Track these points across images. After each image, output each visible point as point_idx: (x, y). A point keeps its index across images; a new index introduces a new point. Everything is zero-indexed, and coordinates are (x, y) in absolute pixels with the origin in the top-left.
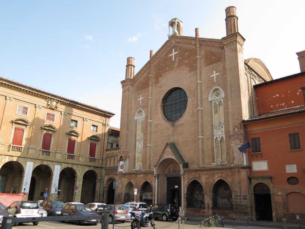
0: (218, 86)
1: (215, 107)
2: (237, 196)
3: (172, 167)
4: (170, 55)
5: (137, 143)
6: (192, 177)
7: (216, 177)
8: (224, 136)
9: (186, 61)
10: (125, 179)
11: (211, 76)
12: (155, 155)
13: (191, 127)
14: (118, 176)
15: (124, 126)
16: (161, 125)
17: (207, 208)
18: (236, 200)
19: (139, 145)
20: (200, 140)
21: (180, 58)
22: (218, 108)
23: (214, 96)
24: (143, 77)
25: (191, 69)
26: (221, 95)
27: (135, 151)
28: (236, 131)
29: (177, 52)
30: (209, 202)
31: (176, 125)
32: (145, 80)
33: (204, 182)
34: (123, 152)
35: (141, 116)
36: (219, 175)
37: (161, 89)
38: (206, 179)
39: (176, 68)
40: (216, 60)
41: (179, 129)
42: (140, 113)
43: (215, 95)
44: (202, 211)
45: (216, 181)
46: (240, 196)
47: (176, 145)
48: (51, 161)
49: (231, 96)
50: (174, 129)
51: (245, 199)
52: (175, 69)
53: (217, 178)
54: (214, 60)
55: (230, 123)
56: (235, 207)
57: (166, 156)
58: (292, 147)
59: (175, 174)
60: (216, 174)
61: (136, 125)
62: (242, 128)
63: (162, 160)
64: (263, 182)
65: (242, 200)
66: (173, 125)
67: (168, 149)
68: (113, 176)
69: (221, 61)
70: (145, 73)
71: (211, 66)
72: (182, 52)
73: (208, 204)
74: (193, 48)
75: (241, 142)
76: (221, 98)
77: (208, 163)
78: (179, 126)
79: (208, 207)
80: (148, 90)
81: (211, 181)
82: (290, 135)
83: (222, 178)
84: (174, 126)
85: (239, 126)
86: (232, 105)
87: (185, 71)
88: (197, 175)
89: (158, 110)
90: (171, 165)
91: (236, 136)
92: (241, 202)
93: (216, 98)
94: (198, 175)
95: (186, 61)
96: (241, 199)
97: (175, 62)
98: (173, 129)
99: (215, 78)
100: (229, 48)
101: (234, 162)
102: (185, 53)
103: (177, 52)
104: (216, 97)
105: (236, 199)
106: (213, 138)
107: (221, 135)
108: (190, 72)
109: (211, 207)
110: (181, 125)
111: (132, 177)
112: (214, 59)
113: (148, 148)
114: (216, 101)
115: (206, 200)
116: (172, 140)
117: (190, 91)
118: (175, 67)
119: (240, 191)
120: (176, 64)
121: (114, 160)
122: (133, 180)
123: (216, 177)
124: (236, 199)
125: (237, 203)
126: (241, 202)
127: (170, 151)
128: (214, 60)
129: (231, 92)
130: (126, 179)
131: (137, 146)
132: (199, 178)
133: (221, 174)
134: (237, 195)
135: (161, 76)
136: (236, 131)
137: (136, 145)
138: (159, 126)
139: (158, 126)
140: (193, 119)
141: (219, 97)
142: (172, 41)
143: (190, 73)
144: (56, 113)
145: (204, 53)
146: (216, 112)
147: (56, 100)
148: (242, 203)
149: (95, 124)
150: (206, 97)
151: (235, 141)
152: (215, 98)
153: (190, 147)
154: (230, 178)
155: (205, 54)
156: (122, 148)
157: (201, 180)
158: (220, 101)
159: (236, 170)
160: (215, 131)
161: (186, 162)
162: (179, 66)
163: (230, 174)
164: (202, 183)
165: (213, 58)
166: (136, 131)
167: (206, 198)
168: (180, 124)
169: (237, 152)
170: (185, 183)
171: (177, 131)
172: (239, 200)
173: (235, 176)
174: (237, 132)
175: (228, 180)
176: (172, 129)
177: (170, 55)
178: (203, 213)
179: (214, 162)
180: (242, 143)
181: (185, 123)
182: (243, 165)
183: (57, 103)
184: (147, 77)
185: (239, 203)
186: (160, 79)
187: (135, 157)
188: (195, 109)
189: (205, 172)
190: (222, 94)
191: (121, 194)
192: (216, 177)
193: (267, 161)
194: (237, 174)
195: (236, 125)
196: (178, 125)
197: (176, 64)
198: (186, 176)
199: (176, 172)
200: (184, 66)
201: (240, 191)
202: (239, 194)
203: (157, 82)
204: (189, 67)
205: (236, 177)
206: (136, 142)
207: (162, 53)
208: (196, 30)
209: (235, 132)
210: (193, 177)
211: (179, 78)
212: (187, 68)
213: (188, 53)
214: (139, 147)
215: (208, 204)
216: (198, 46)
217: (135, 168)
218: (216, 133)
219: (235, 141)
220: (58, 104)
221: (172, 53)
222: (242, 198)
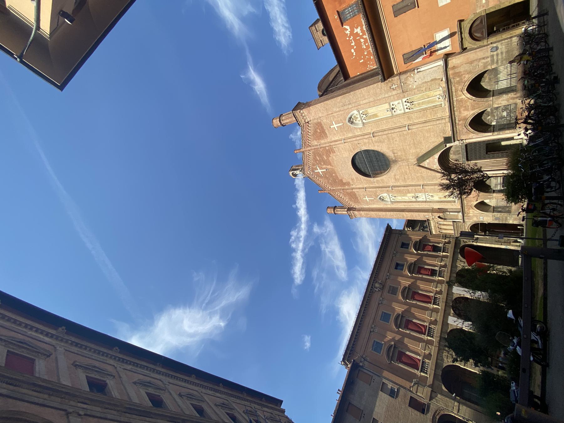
1: (370, 119)
2: (492, 61)
4: (321, 174)
6: (465, 128)
7: (464, 97)
9: (325, 157)
11: (336, 129)
12: (434, 178)
13: (396, 141)
15: (399, 215)
16: (395, 175)
19: (422, 198)
23: (357, 121)
25: (332, 152)
29: (318, 168)
30: (504, 98)
31: (394, 159)
33: (472, 112)
34: (432, 216)
36: (460, 93)
37: (355, 179)
38: (466, 109)
39: (332, 166)
40: (320, 127)
41: (399, 154)
46: (493, 57)
47: (420, 155)
48: (447, 296)
51: (497, 48)
52: (334, 168)
55: (387, 95)
57: (437, 166)
58: (413, 7)
59: (461, 151)
60: (458, 98)
61: (397, 202)
62: (392, 80)
64: (467, 31)
65: (499, 51)
66: (395, 161)
67: (426, 163)
68: (467, 226)
69: (320, 122)
71: (326, 131)
73: (508, 100)
75: (411, 76)
78: (396, 155)
80: (358, 192)
83: (464, 89)
84: (395, 161)
85: (390, 84)
86: (365, 99)
89: (378, 181)
91: (402, 84)
94: (461, 122)
95: (325, 157)
98: (400, 161)
100: (307, 117)
101: (439, 79)
102: (318, 160)
103: (318, 168)
104: (358, 119)
105: (497, 61)
106: (407, 112)
107: (403, 104)
108: (335, 152)
109: (512, 95)
110: (394, 153)
112: (320, 130)
117: (354, 149)
118: (332, 167)
119: (484, 58)
120: (329, 167)
121: (444, 225)
122: (472, 203)
124: (497, 61)
126: (502, 53)
127: (427, 161)
129: (350, 104)
131: (425, 200)
133: (459, 91)
134: (491, 60)
135: (341, 180)
136: (396, 86)
138: (397, 177)
139: (396, 178)
140: (386, 141)
144: (388, 283)
146: (375, 115)
147: (373, 282)
148: (504, 50)
149: (400, 244)
150: (359, 130)
151: (410, 85)
152: (359, 121)
153: (422, 139)
155: (316, 140)
156: (427, 216)
157: (469, 116)
160: (398, 112)
161: (443, 140)
162: (330, 164)
164: (474, 114)
165: (319, 131)
166: (405, 202)
168: (393, 155)
169: (425, 78)
171: (401, 156)
172: (500, 57)
173: (460, 72)
174: (398, 85)
175: (468, 78)
176: (400, 162)
177: (321, 174)
179: (441, 104)
180: (412, 75)
182: (442, 65)
183: (376, 282)
185: (504, 55)
186: (344, 181)
188: (373, 140)
191: (495, 216)
192: (464, 97)
193: (434, 34)
194: (457, 70)
195: (389, 88)
197: (329, 167)
198: (463, 137)
199: (458, 151)
200: (330, 158)
201: (484, 58)
202: (489, 59)
203: (348, 184)
204: (330, 153)
206: (419, 202)
209: (398, 86)
210: (464, 127)
211: (341, 162)
213: (317, 157)
214: (426, 197)
215: (508, 100)
216: (309, 148)
218: (400, 110)
219: (410, 85)
220: (378, 281)
221: (319, 172)
222: (495, 53)
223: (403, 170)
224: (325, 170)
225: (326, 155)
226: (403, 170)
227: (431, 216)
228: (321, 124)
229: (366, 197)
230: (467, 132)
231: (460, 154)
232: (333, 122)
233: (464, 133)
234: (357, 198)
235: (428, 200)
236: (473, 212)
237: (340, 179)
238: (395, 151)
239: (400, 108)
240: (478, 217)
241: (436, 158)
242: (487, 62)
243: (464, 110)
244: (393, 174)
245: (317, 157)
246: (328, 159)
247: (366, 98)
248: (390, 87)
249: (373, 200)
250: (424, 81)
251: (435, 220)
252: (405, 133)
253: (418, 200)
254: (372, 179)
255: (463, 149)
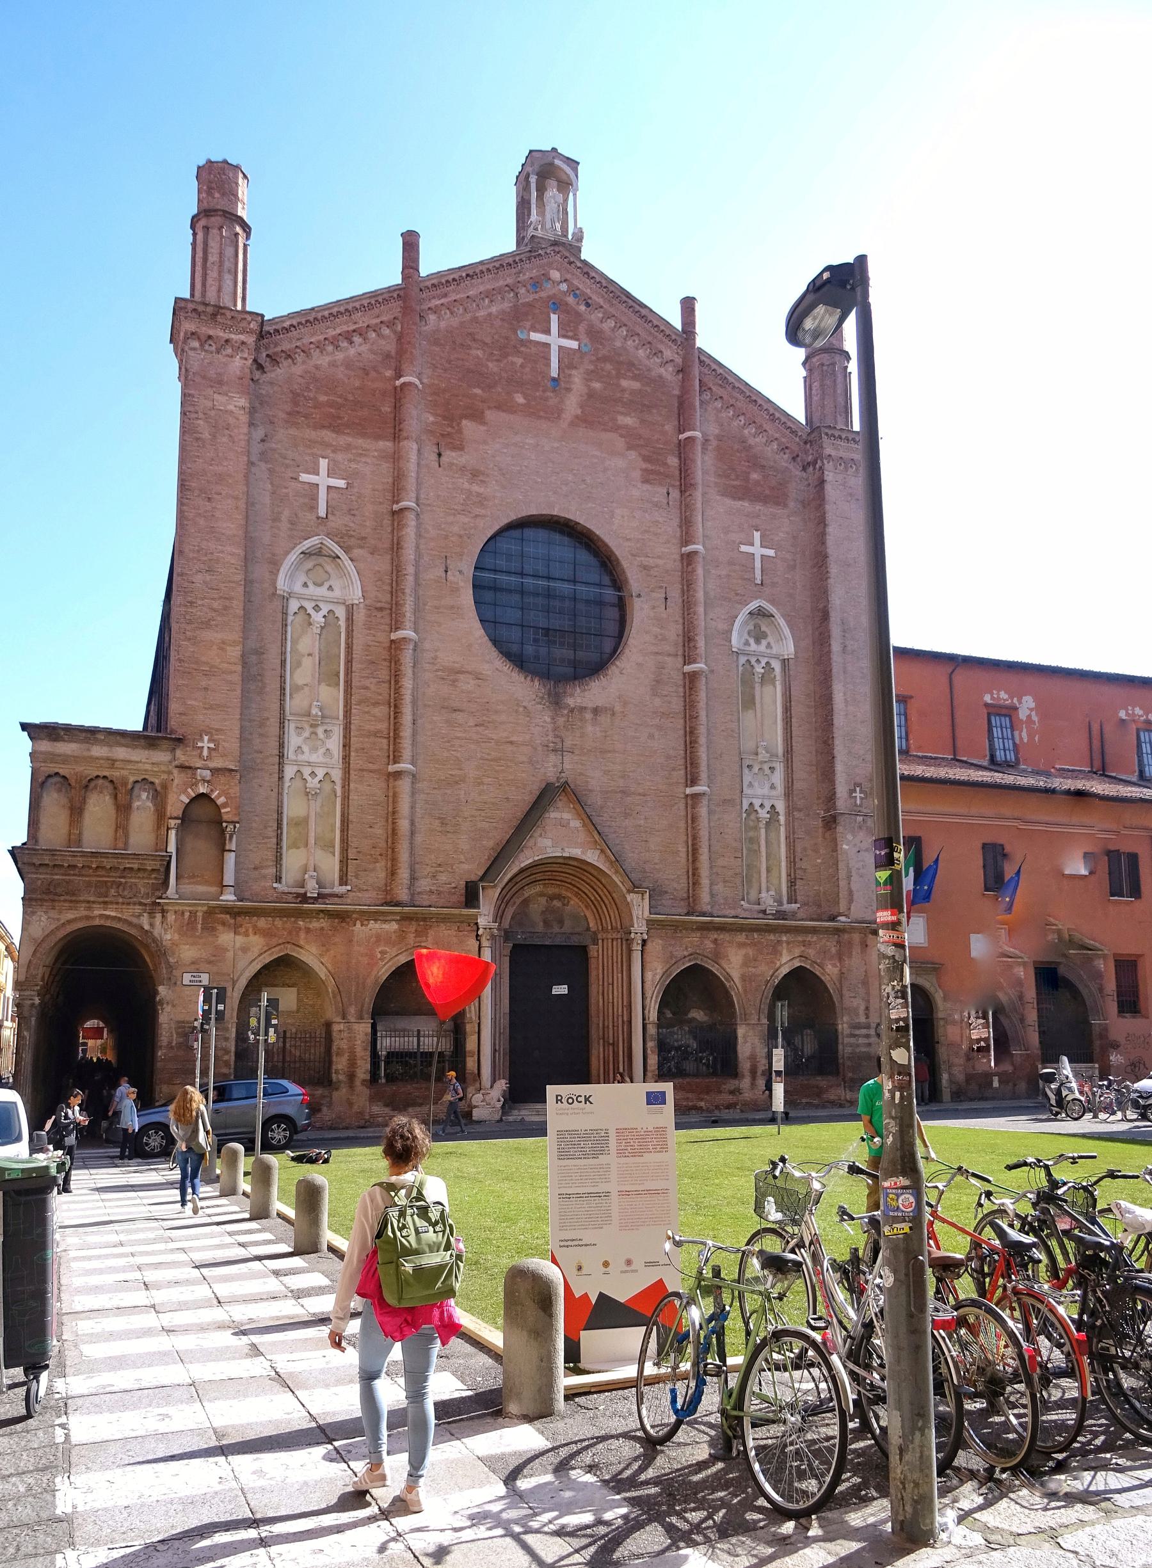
0: (772, 602)
2: (858, 1026)
3: (543, 900)
5: (294, 740)
6: (686, 953)
7: (784, 960)
8: (781, 807)
9: (628, 421)
10: (237, 937)
11: (744, 548)
13: (651, 736)
14: (171, 917)
15: (215, 605)
16: (478, 676)
17: (747, 1073)
18: (852, 1040)
19: (306, 749)
20: (705, 801)
21: (597, 385)
22: (757, 687)
23: (746, 636)
24: (340, 356)
25: (652, 472)
26: (770, 639)
27: (281, 778)
28: (858, 802)
30: (758, 1050)
31: (571, 701)
32: (357, 384)
33: (736, 975)
34: (215, 771)
35: (318, 584)
36: (797, 952)
37: (475, 488)
38: (745, 964)
39: (572, 424)
40: (767, 492)
41: (589, 729)
42: (309, 564)
43: (749, 633)
44: (732, 1084)
45: (785, 970)
49: (845, 668)
50: (561, 721)
53: (786, 962)
54: (759, 489)
56: (849, 1063)
59: (556, 929)
63: (525, 859)
65: (874, 1040)
66: (556, 701)
68: (135, 920)
69: (785, 506)
70: (357, 339)
72: (605, 359)
73: (753, 1058)
74: (660, 377)
76: (768, 651)
77: (726, 899)
79: (753, 1072)
81: (763, 970)
82: (984, 846)
85: (867, 785)
87: (620, 463)
88: (709, 945)
89: (455, 590)
90: (538, 888)
91: (860, 819)
92: (869, 1045)
93: (753, 646)
95: (628, 421)
96: (868, 1036)
97: (568, 390)
99: (758, 564)
102: (619, 376)
104: (752, 641)
105: (854, 1036)
107: (769, 798)
108: (646, 481)
110: (596, 711)
111: (308, 930)
112: (757, 483)
113: (404, 785)
114: (753, 660)
115: (746, 1042)
116: (549, 769)
117: (646, 568)
119: (867, 1008)
123: (785, 958)
124: (854, 1036)
125: (858, 1050)
128: (759, 489)
130: (256, 942)
132: (717, 957)
135: (477, 416)
136: (858, 802)
137: (281, 745)
138: (467, 684)
139: (461, 677)
140: (657, 701)
141: (762, 648)
142: (550, 265)
143: (646, 487)
145: (717, 431)
146: (749, 702)
151: (854, 836)
152: (747, 643)
153: (642, 822)
154: (834, 966)
157: (725, 966)
158: (767, 663)
159: (856, 937)
162: (585, 420)
163: (833, 950)
164: (729, 977)
165: (755, 476)
166: (283, 663)
167: (745, 1037)
168: (590, 705)
170: (649, 975)
172: (861, 1041)
173: (850, 956)
174: (861, 806)
175: (829, 972)
176: (548, 720)
178: (732, 1092)
181: (618, 708)
184: (373, 374)
185: (864, 1049)
186: (469, 427)
187: (280, 813)
188: (669, 660)
189: (741, 938)
190: (781, 638)
192: (784, 960)
194: (856, 951)
195: (858, 780)
196: (582, 709)
197: (572, 405)
198: (656, 946)
199: (561, 922)
200: (620, 443)
202: (862, 1019)
204: (646, 459)
205: (855, 961)
207: (489, 295)
208: (688, 306)
209: (856, 805)
211: (588, 480)
212: (633, 455)
213: (636, 385)
214: (309, 764)
217: (278, 879)
219: (854, 836)
223: (503, 717)
224: (554, 373)
225: (640, 437)
226: (503, 717)
227: (212, 765)
228: (778, 504)
229: (341, 483)
230: (672, 956)
231: (546, 923)
232: (771, 553)
233: (670, 948)
234: (337, 429)
235: (289, 771)
236: (245, 950)
237: (490, 415)
238: (604, 719)
239: (756, 784)
240: (204, 967)
241: (583, 853)
242: (857, 1015)
243: (746, 956)
244: (486, 669)
245: (636, 385)
246: (616, 428)
247: (851, 708)
248: (860, 785)
249: (314, 508)
250: (854, 873)
251: (178, 778)
252: (675, 773)
253: (291, 728)
254: (466, 567)
255: (569, 938)
